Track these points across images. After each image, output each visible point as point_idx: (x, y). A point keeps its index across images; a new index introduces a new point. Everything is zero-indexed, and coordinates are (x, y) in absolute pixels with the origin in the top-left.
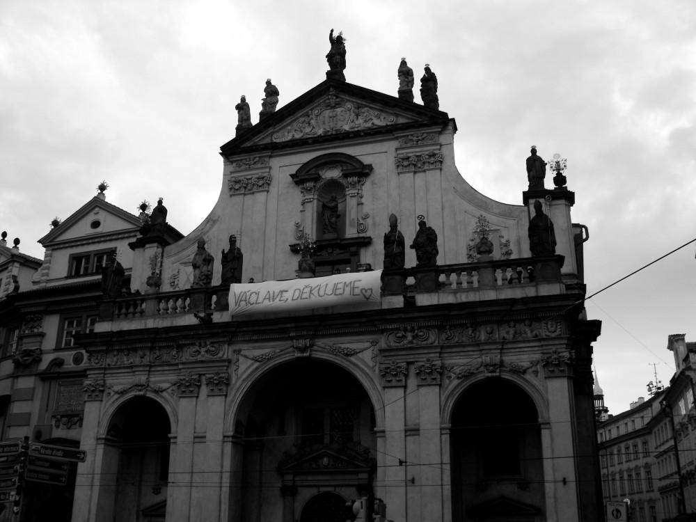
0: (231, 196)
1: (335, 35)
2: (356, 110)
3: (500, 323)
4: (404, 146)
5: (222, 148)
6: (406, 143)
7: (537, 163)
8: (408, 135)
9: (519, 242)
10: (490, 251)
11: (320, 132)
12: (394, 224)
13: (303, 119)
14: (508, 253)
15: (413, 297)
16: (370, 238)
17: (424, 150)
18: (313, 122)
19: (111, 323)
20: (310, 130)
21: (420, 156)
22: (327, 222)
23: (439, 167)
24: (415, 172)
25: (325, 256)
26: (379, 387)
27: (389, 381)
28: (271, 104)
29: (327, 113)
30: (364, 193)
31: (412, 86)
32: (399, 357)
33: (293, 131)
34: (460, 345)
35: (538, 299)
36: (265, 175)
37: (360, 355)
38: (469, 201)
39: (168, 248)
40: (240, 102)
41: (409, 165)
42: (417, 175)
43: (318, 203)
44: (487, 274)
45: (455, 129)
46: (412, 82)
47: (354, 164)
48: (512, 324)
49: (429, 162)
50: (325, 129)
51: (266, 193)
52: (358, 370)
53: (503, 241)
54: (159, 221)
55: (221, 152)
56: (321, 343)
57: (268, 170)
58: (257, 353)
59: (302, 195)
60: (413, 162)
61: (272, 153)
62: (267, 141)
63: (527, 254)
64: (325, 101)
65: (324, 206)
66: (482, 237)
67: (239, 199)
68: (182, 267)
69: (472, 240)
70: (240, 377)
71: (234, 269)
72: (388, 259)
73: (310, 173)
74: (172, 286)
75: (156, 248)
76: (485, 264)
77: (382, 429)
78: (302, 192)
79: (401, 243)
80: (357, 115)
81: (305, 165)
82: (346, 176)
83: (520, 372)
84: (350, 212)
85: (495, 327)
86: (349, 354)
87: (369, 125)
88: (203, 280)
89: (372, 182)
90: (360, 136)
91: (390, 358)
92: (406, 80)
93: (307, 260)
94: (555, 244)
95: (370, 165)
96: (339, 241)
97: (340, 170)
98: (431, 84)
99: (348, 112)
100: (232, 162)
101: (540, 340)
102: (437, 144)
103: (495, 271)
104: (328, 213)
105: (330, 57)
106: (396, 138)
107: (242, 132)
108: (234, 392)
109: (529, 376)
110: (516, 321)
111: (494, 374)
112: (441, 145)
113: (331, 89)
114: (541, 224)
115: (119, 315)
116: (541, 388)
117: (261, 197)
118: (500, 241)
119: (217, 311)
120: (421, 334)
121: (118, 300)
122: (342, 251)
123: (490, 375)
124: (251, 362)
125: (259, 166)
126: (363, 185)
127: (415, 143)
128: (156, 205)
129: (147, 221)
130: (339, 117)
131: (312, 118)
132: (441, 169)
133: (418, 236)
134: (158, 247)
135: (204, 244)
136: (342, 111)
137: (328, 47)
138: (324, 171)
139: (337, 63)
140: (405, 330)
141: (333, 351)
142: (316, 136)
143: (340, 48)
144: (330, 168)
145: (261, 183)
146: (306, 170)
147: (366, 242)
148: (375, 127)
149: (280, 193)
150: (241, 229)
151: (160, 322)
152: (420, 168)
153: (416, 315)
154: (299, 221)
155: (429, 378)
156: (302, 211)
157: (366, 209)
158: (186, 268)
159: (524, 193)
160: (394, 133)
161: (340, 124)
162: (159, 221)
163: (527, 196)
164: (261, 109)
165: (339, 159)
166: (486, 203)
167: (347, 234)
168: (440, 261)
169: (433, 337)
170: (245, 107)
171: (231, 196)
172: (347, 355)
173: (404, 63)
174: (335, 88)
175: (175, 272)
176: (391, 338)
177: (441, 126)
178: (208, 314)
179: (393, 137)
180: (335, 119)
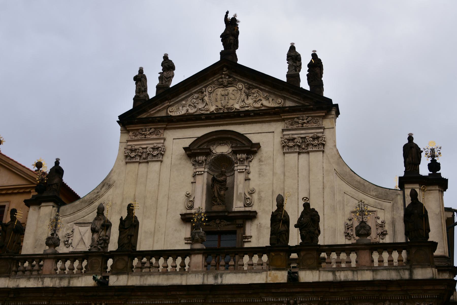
0: (127, 163)
1: (230, 16)
2: (246, 91)
4: (290, 127)
5: (120, 117)
6: (292, 125)
7: (414, 150)
8: (294, 118)
9: (393, 223)
10: (368, 234)
11: (212, 108)
12: (280, 202)
13: (196, 95)
14: (384, 234)
15: (297, 273)
16: (255, 212)
17: (309, 133)
18: (206, 98)
19: (8, 278)
20: (203, 106)
21: (305, 138)
22: (216, 195)
23: (322, 149)
24: (299, 153)
25: (213, 227)
28: (167, 78)
29: (220, 91)
30: (251, 170)
31: (300, 71)
33: (187, 105)
35: (412, 282)
36: (160, 145)
38: (348, 183)
39: (62, 208)
40: (137, 73)
41: (294, 146)
43: (208, 176)
44: (365, 256)
45: (338, 113)
46: (300, 67)
47: (243, 142)
49: (312, 145)
50: (217, 106)
51: (159, 163)
53: (379, 222)
54: (56, 181)
55: (119, 120)
57: (162, 141)
59: (193, 167)
60: (299, 144)
61: (167, 125)
62: (163, 114)
63: (401, 238)
64: (219, 79)
65: (214, 180)
66: (361, 220)
67: (133, 167)
68: (76, 227)
69: (350, 220)
71: (131, 236)
72: (273, 236)
73: (201, 147)
74: (65, 244)
75: (52, 207)
76: (364, 246)
78: (193, 165)
79: (286, 222)
80: (248, 96)
81: (199, 139)
84: (237, 186)
87: (258, 105)
88: (101, 244)
89: (260, 159)
90: (250, 116)
92: (295, 64)
93: (199, 233)
94: (429, 231)
95: (258, 144)
96: (227, 214)
97: (229, 148)
98: (317, 70)
99: (239, 92)
100: (128, 132)
102: (321, 128)
103: (372, 253)
104: (217, 186)
105: (224, 37)
106: (283, 120)
107: (139, 103)
110: (390, 301)
112: (324, 129)
113: (225, 69)
114: (416, 211)
115: (16, 272)
117: (155, 166)
118: (376, 222)
119: (113, 274)
121: (16, 257)
122: (228, 223)
125: (154, 136)
126: (250, 161)
128: (53, 165)
129: (43, 180)
130: (231, 96)
131: (206, 95)
132: (323, 152)
133: (302, 216)
134: (53, 207)
135: (103, 210)
136: (234, 90)
137: (222, 28)
138: (215, 147)
139: (231, 43)
142: (208, 112)
143: (234, 29)
144: (221, 143)
145: (155, 153)
146: (197, 146)
147: (252, 216)
148: (263, 108)
149: (173, 162)
150: (135, 195)
151: (58, 281)
152: (303, 149)
154: (190, 191)
156: (192, 183)
157: (253, 184)
158: (79, 227)
159: (400, 178)
160: (281, 115)
161: (231, 102)
162: (56, 181)
163: (402, 182)
164: (157, 82)
165: (229, 136)
166: (364, 185)
167: (234, 206)
168: (322, 240)
170: (143, 79)
171: (127, 163)
173: (292, 48)
174: (228, 68)
175: (69, 232)
177: (326, 111)
178: (103, 276)
179: (280, 118)
180: (226, 97)
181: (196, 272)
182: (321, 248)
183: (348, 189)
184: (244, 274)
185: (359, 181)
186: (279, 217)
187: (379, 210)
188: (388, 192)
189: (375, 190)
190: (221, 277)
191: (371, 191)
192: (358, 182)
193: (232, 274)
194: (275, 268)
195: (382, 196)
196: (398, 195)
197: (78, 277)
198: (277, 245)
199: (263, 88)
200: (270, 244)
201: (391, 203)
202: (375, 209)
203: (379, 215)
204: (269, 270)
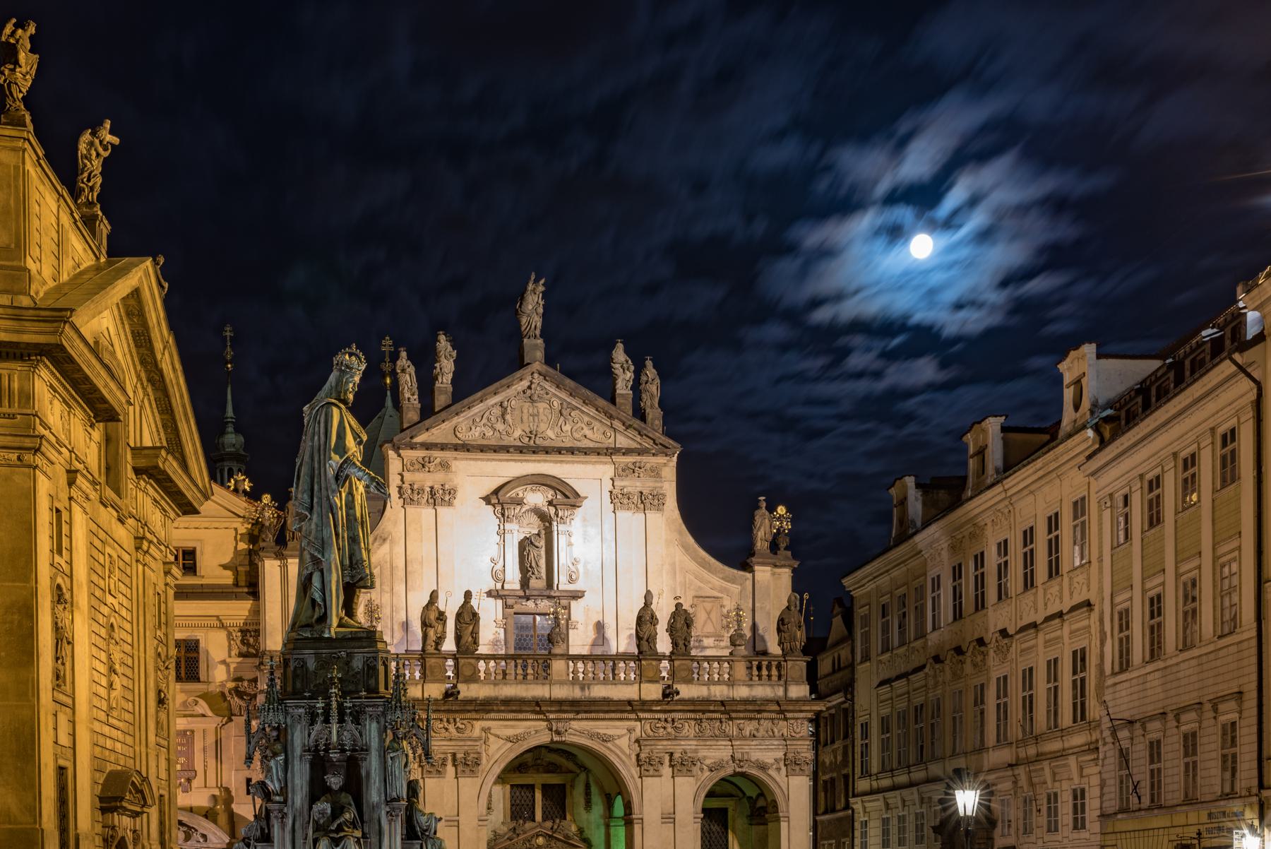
3: (751, 719)
11: (518, 433)
18: (508, 417)
22: (534, 565)
26: (636, 776)
27: (647, 771)
32: (659, 747)
34: (715, 737)
37: (617, 742)
42: (636, 514)
48: (762, 722)
52: (616, 757)
53: (725, 611)
56: (575, 725)
58: (510, 732)
70: (492, 756)
77: (641, 816)
78: (497, 517)
82: (555, 506)
83: (763, 767)
85: (747, 722)
86: (605, 739)
91: (649, 747)
101: (785, 740)
108: (485, 773)
109: (771, 772)
111: (744, 770)
116: (781, 784)
120: (681, 726)
123: (740, 770)
124: (502, 742)
127: (637, 475)
130: (542, 417)
136: (545, 409)
140: (666, 720)
141: (592, 736)
147: (577, 595)
153: (680, 707)
155: (684, 769)
169: (689, 729)
172: (604, 741)
176: (648, 727)
181: (561, 683)
183: (693, 566)
184: (614, 686)
187: (725, 596)
190: (589, 689)
197: (417, 684)
198: (648, 653)
199: (585, 410)
200: (640, 652)
202: (720, 595)
203: (724, 603)
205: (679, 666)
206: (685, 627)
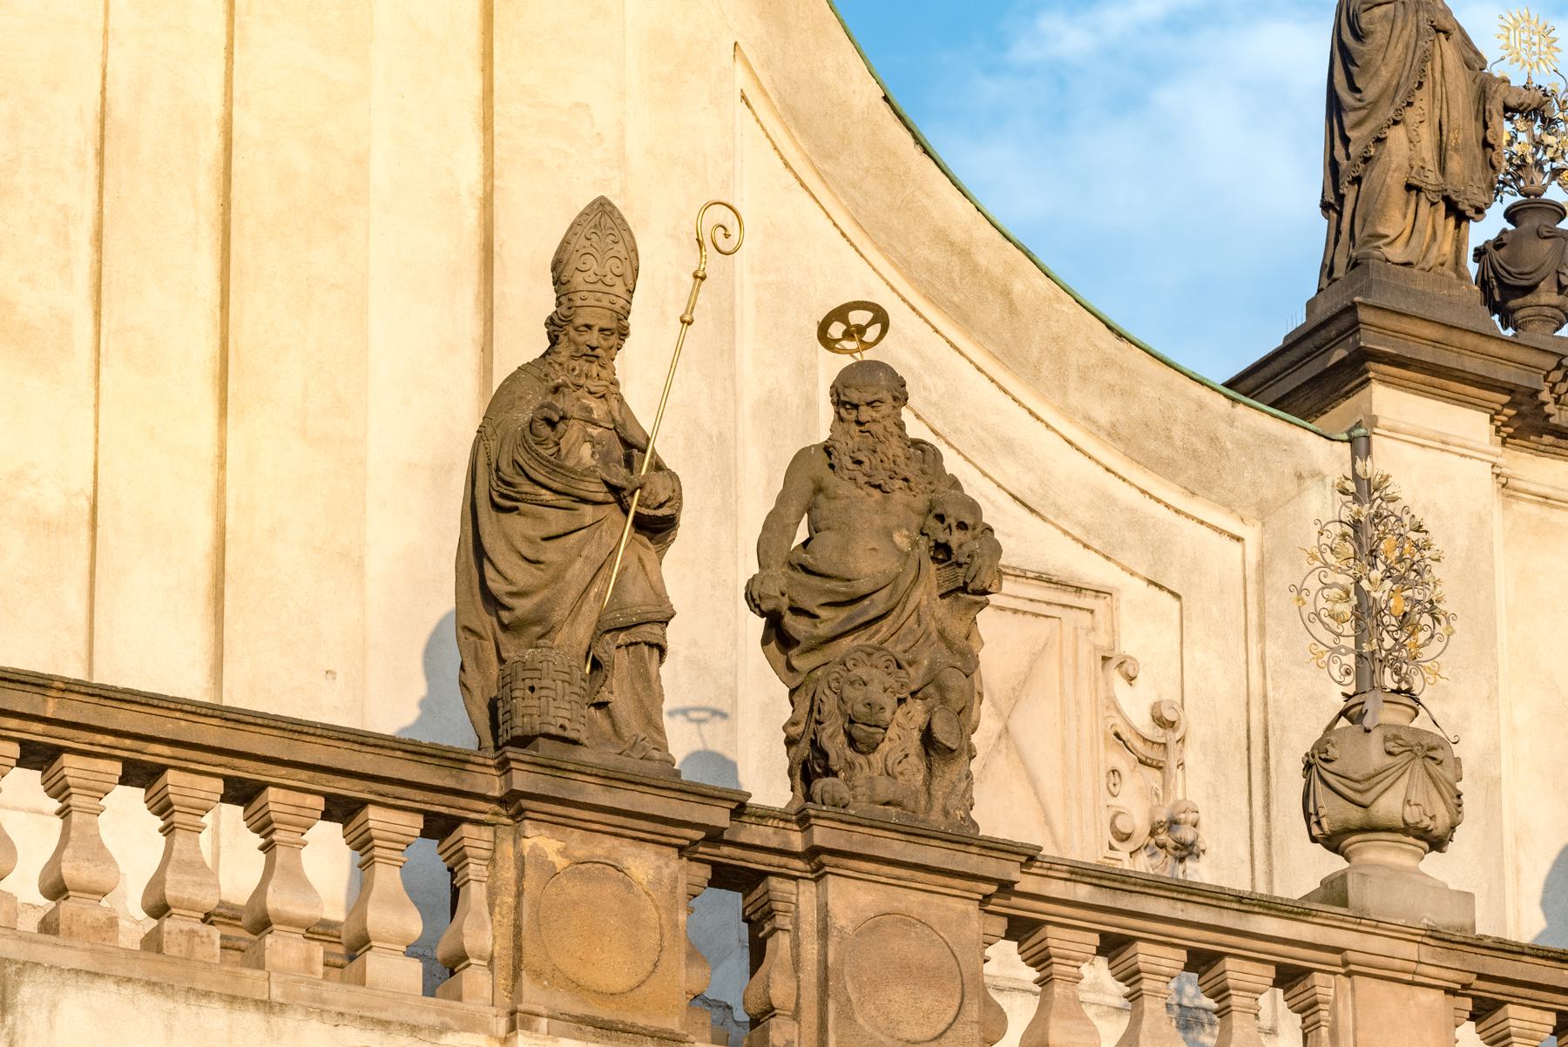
53: (1136, 707)
118: (1114, 705)
166: (1006, 293)
182: (1026, 883)
184: (251, 1019)
185: (958, 235)
186: (586, 450)
188: (1222, 429)
189: (1110, 376)
191: (1073, 376)
192: (952, 244)
193: (127, 990)
194: (579, 1010)
195: (1166, 452)
196: (1308, 483)
201: (1239, 539)
202: (1092, 569)
203: (1129, 645)
204: (517, 1020)
205: (873, 925)
206: (926, 591)
